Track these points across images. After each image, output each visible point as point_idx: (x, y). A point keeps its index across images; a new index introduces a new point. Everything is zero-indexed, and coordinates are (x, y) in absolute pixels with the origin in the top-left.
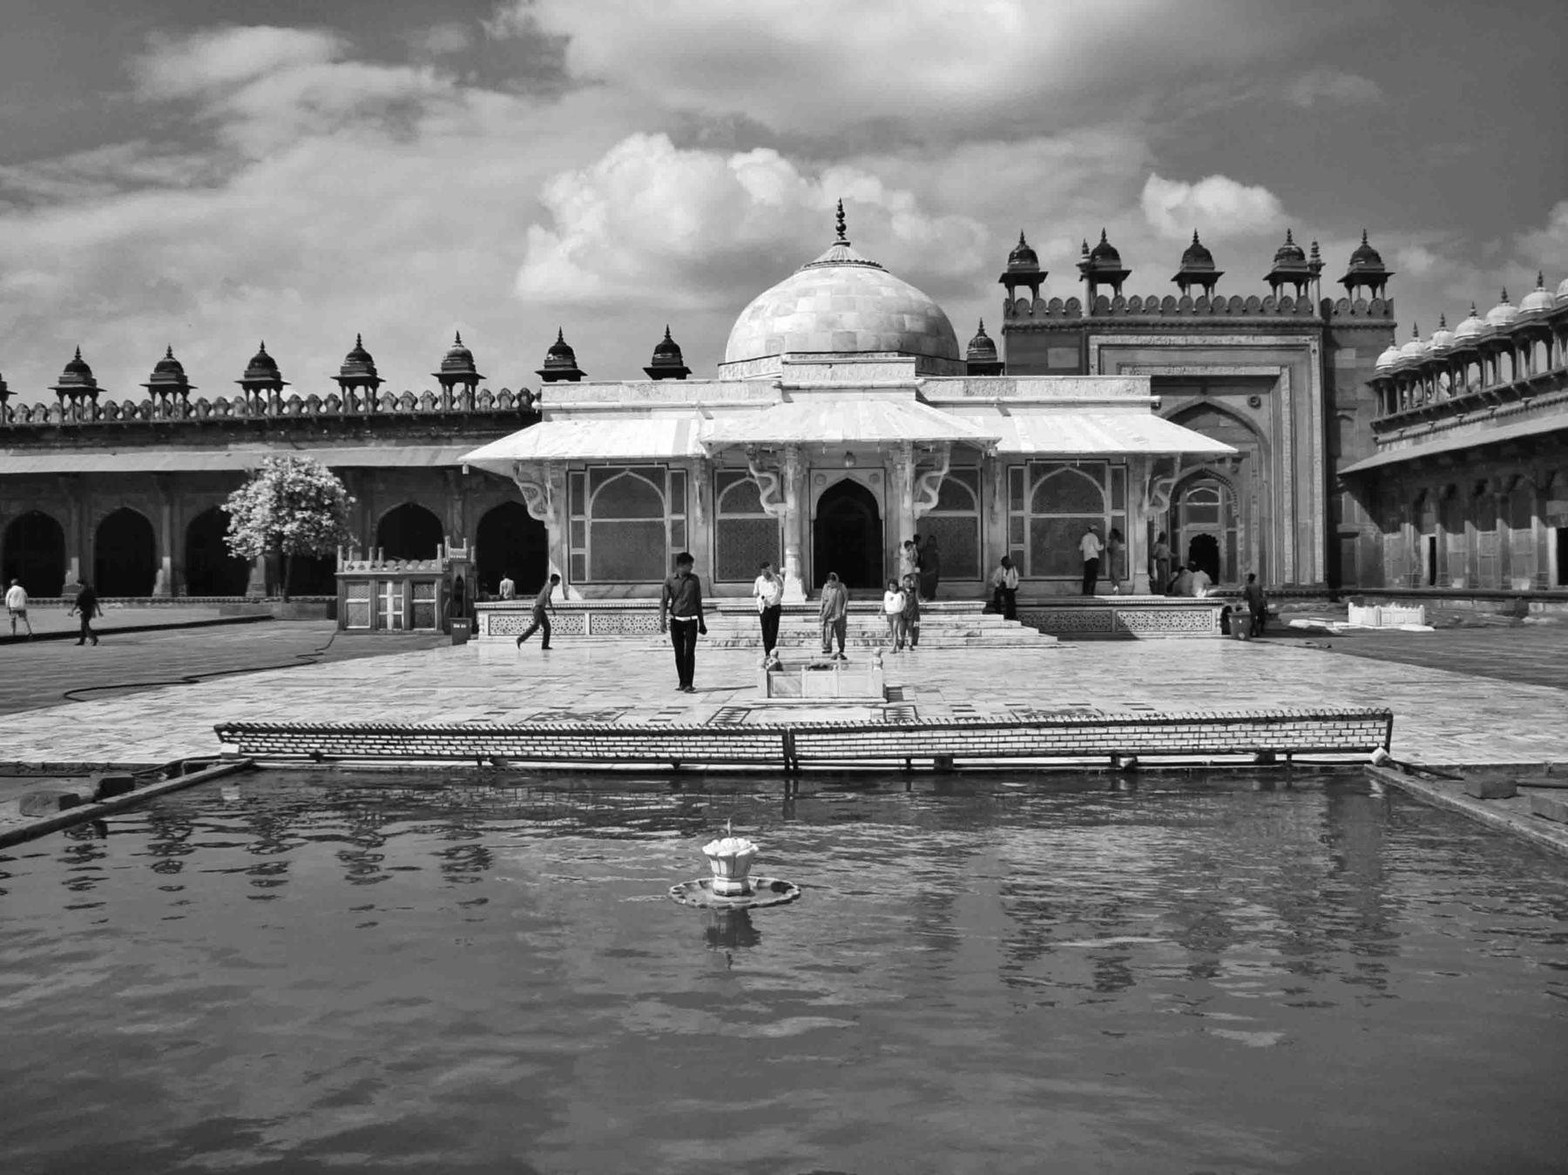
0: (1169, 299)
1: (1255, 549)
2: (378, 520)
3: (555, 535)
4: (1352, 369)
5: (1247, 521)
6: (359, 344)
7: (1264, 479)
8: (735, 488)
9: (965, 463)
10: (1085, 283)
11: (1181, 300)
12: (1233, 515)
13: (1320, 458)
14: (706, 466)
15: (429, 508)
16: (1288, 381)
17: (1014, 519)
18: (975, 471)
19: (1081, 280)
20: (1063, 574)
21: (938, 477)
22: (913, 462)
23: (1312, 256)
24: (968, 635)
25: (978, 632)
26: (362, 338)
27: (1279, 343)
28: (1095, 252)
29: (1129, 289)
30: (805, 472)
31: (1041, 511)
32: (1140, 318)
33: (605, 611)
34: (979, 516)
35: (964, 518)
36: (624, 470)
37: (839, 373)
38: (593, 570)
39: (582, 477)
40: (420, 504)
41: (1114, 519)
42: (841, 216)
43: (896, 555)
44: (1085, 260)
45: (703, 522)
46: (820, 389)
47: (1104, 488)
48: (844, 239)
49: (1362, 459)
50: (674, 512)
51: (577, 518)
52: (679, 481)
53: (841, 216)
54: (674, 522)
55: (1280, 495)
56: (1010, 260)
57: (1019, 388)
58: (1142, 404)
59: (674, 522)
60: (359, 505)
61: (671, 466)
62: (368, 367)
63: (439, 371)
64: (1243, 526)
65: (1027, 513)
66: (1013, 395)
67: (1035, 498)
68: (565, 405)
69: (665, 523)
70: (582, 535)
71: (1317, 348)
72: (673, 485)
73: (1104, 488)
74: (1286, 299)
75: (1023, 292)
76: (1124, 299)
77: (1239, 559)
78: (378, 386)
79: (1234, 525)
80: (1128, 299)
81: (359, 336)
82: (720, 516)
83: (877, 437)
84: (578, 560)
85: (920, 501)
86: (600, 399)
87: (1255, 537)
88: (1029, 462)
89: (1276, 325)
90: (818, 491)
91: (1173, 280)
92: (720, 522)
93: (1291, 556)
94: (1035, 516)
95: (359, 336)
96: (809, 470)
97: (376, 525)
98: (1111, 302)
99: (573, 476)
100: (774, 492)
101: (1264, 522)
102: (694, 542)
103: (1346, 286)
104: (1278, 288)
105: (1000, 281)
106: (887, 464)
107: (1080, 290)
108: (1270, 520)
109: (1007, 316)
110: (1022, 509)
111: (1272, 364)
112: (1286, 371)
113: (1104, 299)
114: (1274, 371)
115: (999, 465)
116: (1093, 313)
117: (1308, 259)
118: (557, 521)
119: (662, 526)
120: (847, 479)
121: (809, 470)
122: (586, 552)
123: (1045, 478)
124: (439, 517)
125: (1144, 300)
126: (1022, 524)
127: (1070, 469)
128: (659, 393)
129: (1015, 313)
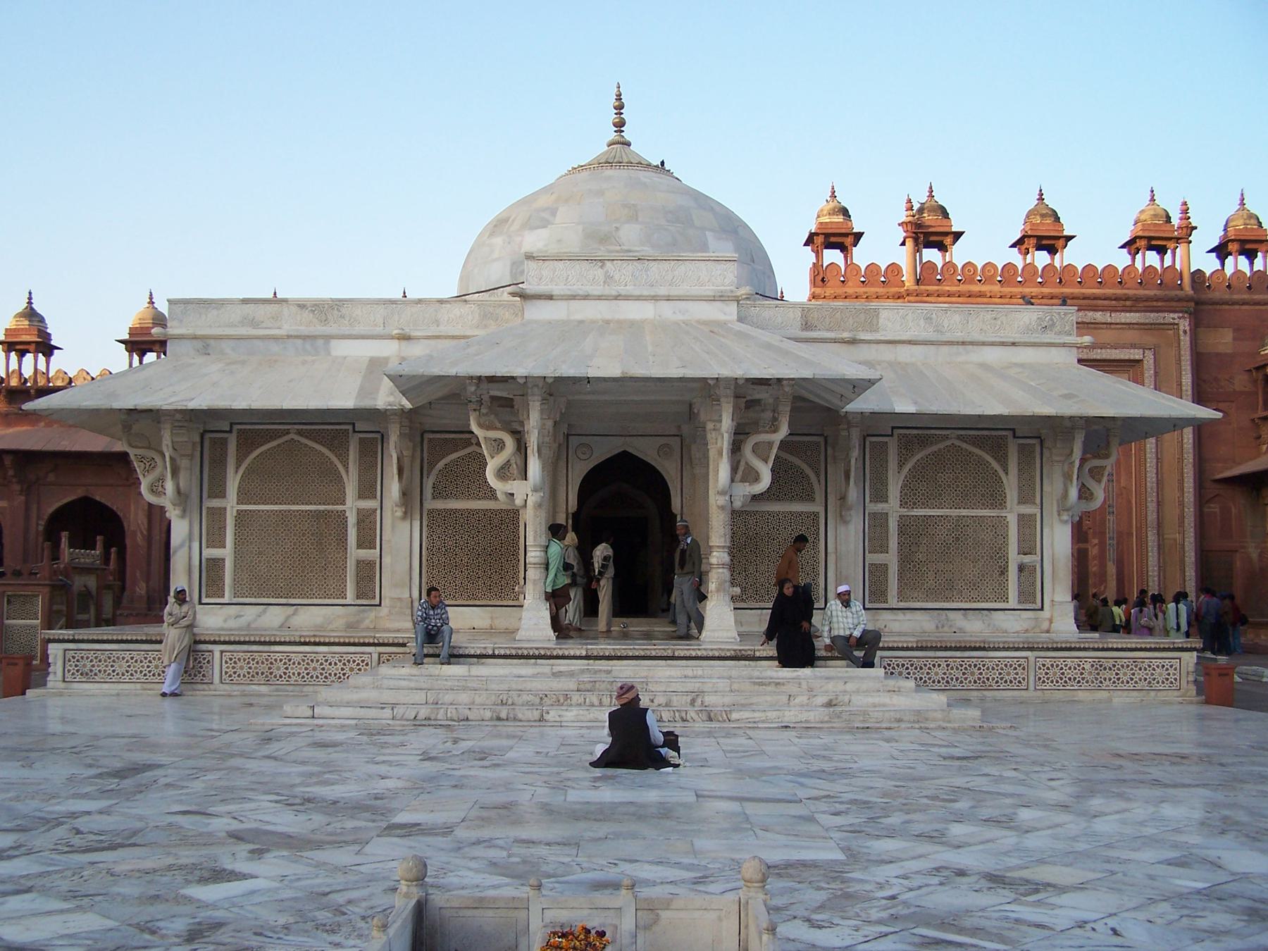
0: (1009, 267)
1: (1112, 569)
2: (46, 517)
3: (180, 530)
4: (1226, 355)
5: (1103, 534)
6: (30, 303)
7: (1123, 484)
8: (456, 460)
9: (806, 432)
10: (909, 243)
11: (1023, 269)
12: (1085, 528)
13: (1191, 460)
14: (411, 428)
15: (109, 504)
16: (1152, 367)
17: (874, 516)
18: (817, 444)
19: (903, 244)
20: (947, 599)
21: (770, 444)
22: (733, 420)
23: (1181, 219)
24: (830, 704)
25: (846, 698)
26: (33, 296)
27: (1142, 321)
28: (921, 210)
29: (960, 254)
30: (561, 438)
31: (914, 506)
32: (976, 288)
33: (245, 647)
34: (821, 510)
35: (801, 514)
36: (288, 432)
37: (617, 277)
38: (235, 581)
39: (224, 443)
40: (98, 498)
41: (1021, 517)
42: (619, 108)
43: (704, 568)
44: (910, 219)
45: (405, 513)
46: (586, 297)
47: (1007, 473)
48: (623, 136)
49: (1239, 464)
50: (361, 496)
51: (216, 503)
52: (372, 449)
53: (619, 108)
54: (359, 511)
55: (1142, 505)
56: (818, 217)
57: (881, 321)
58: (1064, 345)
59: (359, 511)
60: (23, 498)
61: (359, 427)
62: (39, 330)
63: (127, 337)
64: (1096, 541)
65: (893, 507)
66: (877, 331)
67: (904, 486)
68: (199, 332)
69: (347, 514)
70: (223, 528)
71: (1187, 328)
72: (360, 457)
73: (1007, 473)
74: (1149, 269)
75: (833, 256)
76: (954, 266)
77: (1091, 581)
78: (51, 354)
79: (1086, 541)
80: (960, 267)
81: (30, 293)
82: (430, 504)
83: (674, 372)
84: (214, 567)
85: (741, 481)
86: (254, 323)
87: (1111, 554)
88: (897, 432)
89: (1137, 299)
90: (578, 472)
91: (1011, 247)
92: (430, 512)
93: (1156, 579)
94: (904, 511)
95: (30, 293)
96: (568, 435)
97: (42, 523)
98: (939, 267)
99: (213, 441)
100: (507, 464)
101: (1123, 537)
102: (389, 541)
103: (1218, 257)
104: (1139, 257)
105: (806, 244)
106: (686, 429)
107: (902, 257)
108: (1130, 534)
109: (814, 283)
110: (884, 499)
111: (1133, 346)
112: (1150, 356)
113: (930, 266)
114: (1136, 354)
115: (855, 435)
116: (918, 282)
117: (1175, 221)
118: (184, 511)
119: (342, 516)
120: (625, 454)
121: (568, 436)
122: (226, 553)
123: (918, 457)
124: (121, 515)
125: (979, 268)
126: (885, 525)
127: (957, 443)
128: (342, 317)
129: (823, 280)
